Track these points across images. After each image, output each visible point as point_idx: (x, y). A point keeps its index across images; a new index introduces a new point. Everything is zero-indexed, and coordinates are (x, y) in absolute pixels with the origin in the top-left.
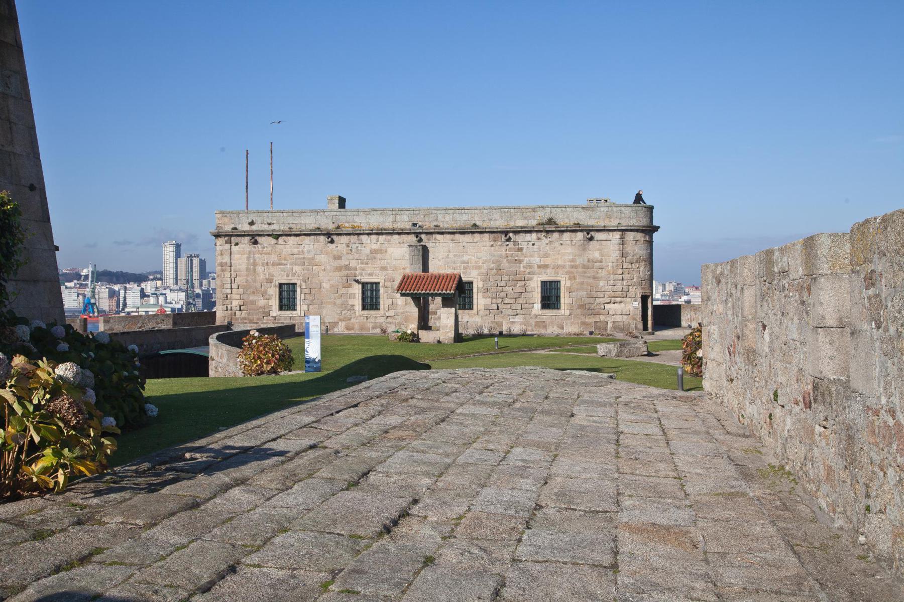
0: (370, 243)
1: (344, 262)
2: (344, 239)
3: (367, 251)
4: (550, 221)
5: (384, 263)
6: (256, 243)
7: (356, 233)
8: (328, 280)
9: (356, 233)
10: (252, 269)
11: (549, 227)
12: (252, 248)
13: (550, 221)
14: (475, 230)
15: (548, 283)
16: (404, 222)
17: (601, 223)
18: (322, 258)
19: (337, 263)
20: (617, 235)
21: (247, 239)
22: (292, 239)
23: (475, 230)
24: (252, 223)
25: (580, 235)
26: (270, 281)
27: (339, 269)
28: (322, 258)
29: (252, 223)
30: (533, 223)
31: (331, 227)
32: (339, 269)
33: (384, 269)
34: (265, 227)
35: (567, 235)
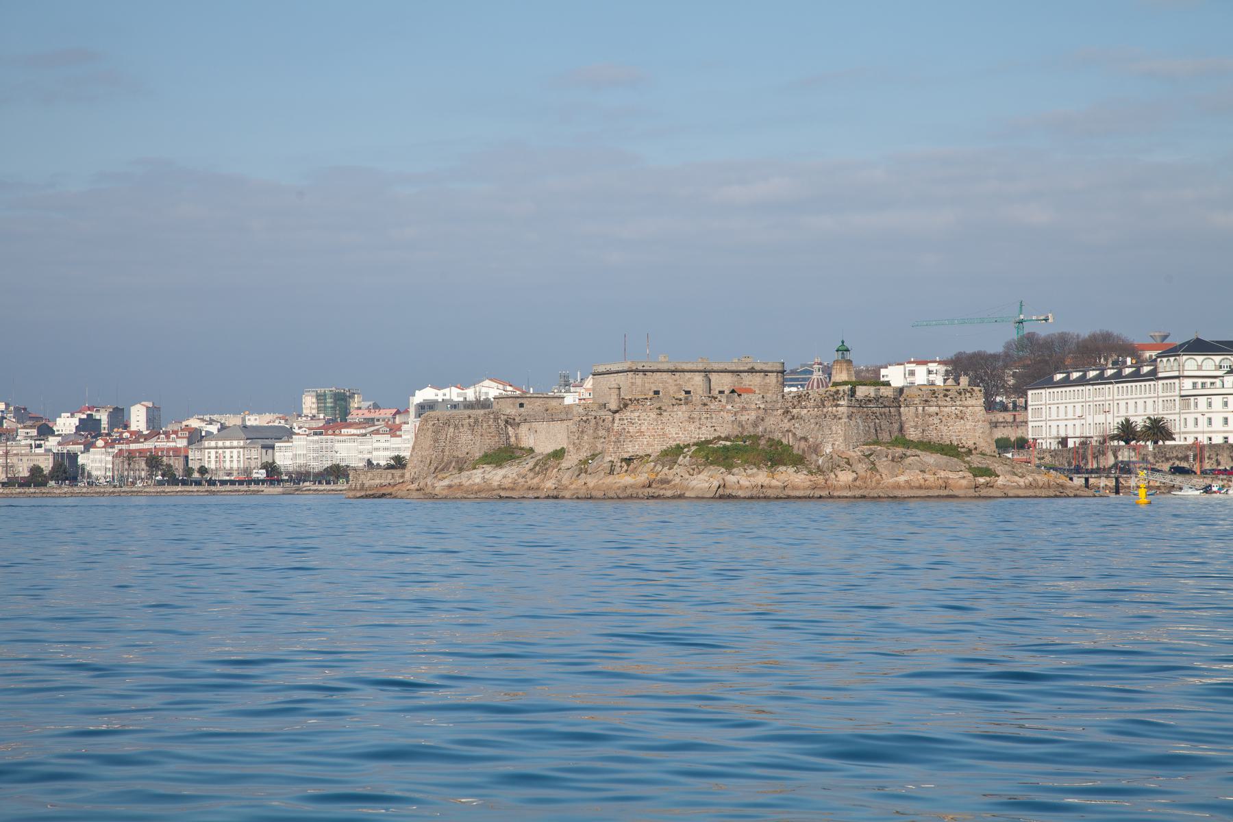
0: (688, 375)
1: (678, 382)
2: (678, 374)
3: (687, 378)
4: (753, 368)
5: (693, 383)
6: (645, 375)
7: (683, 371)
8: (672, 390)
9: (683, 371)
10: (643, 385)
11: (752, 371)
12: (644, 376)
13: (753, 368)
14: (726, 371)
15: (319, 405)
16: (701, 367)
17: (770, 369)
18: (670, 381)
19: (676, 383)
20: (775, 374)
21: (641, 373)
22: (658, 373)
23: (726, 371)
24: (643, 366)
25: (763, 374)
26: (650, 390)
27: (676, 385)
28: (670, 381)
29: (643, 366)
30: (746, 368)
31: (673, 368)
32: (676, 385)
33: (693, 385)
34: (648, 368)
35: (758, 374)
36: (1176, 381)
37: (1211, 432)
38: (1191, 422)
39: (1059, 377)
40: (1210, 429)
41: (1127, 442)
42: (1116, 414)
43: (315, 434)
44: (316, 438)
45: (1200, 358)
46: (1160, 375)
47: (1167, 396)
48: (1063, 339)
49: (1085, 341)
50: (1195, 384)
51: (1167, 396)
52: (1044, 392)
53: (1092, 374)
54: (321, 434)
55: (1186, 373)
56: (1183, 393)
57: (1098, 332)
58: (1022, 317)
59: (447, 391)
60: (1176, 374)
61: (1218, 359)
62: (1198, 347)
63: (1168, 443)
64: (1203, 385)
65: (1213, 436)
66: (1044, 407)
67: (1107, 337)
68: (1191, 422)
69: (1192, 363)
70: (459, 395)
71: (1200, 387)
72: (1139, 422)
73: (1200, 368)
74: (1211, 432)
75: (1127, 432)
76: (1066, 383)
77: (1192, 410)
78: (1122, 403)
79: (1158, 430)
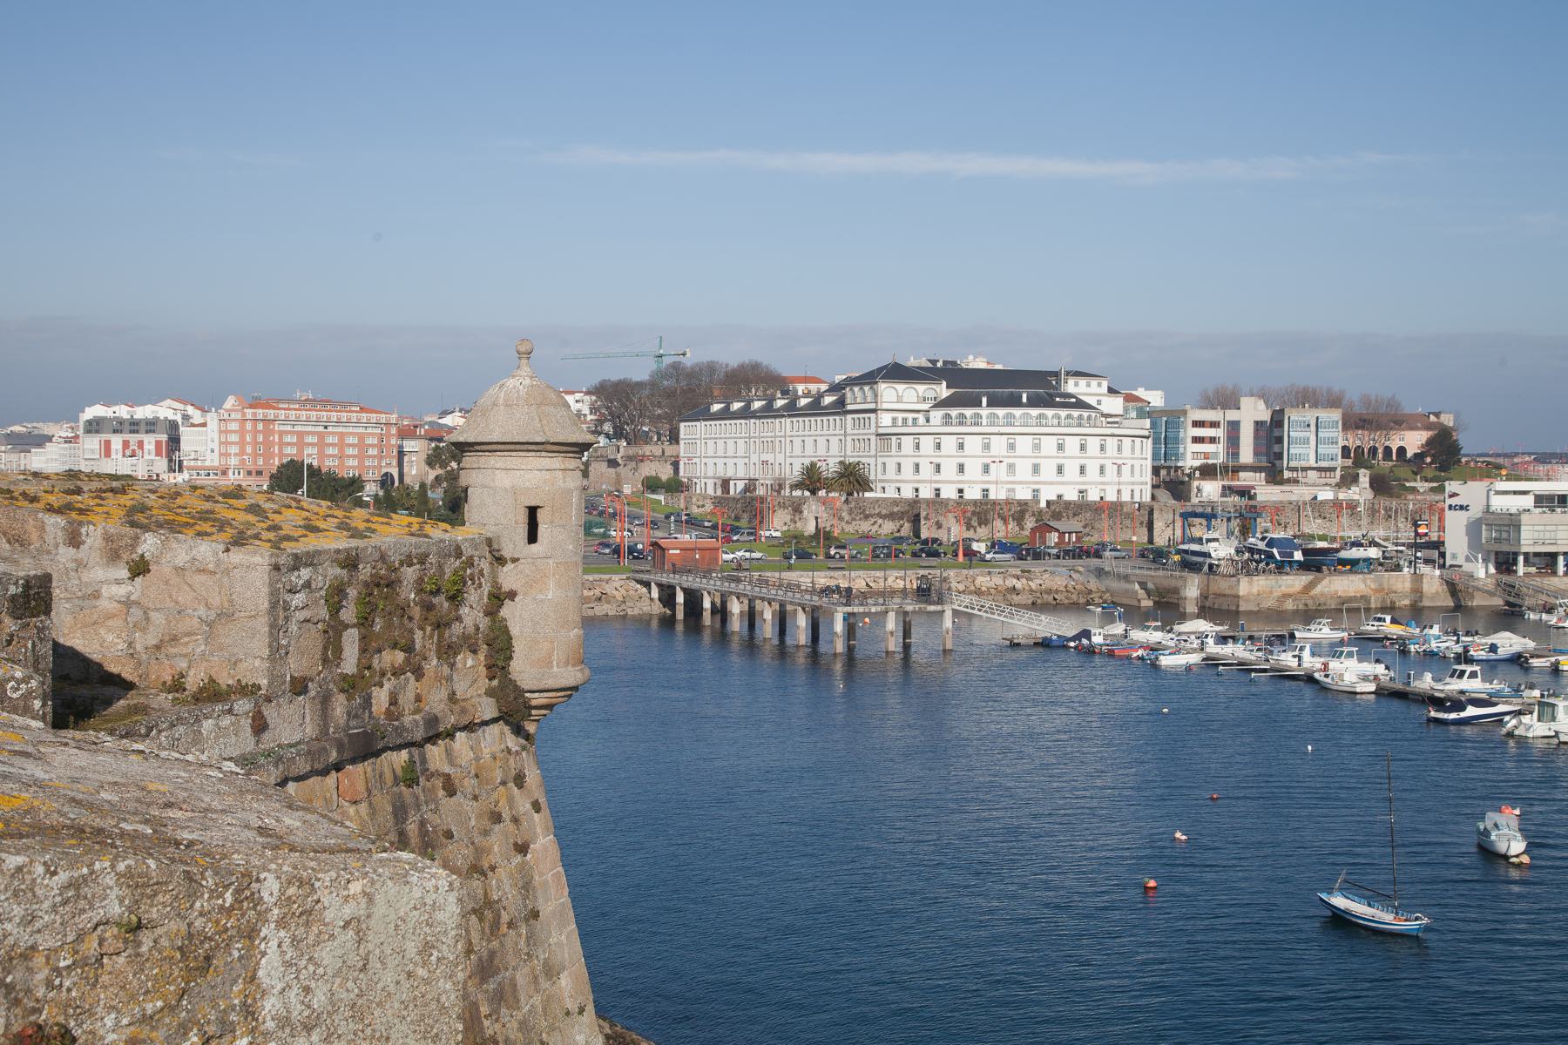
36: (873, 416)
37: (919, 482)
38: (891, 467)
39: (716, 407)
40: (916, 478)
41: (813, 492)
42: (788, 454)
43: (66, 442)
44: (67, 445)
45: (901, 387)
46: (849, 407)
47: (859, 434)
48: (711, 368)
49: (734, 370)
50: (894, 419)
51: (859, 434)
52: (700, 426)
53: (736, 406)
54: (70, 442)
55: (885, 406)
56: (881, 431)
57: (747, 362)
58: (662, 352)
59: (116, 408)
60: (872, 406)
61: (921, 388)
62: (898, 373)
63: (867, 495)
64: (905, 420)
65: (921, 487)
66: (698, 442)
67: (755, 366)
68: (891, 467)
69: (889, 392)
70: (128, 412)
71: (910, 423)
72: (830, 467)
73: (899, 401)
74: (919, 482)
75: (812, 480)
76: (726, 415)
77: (894, 453)
78: (797, 442)
79: (853, 479)
